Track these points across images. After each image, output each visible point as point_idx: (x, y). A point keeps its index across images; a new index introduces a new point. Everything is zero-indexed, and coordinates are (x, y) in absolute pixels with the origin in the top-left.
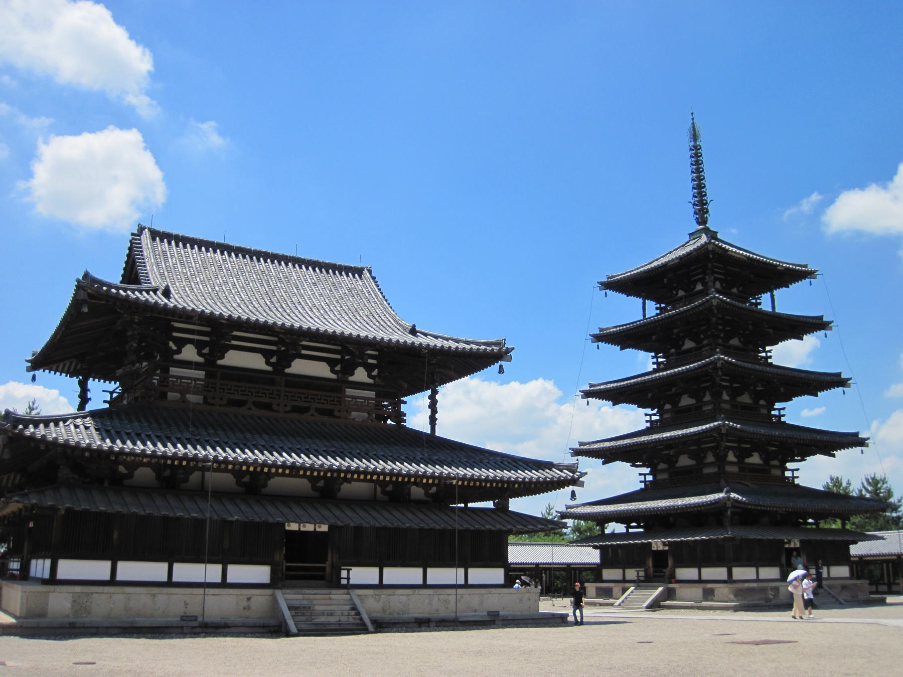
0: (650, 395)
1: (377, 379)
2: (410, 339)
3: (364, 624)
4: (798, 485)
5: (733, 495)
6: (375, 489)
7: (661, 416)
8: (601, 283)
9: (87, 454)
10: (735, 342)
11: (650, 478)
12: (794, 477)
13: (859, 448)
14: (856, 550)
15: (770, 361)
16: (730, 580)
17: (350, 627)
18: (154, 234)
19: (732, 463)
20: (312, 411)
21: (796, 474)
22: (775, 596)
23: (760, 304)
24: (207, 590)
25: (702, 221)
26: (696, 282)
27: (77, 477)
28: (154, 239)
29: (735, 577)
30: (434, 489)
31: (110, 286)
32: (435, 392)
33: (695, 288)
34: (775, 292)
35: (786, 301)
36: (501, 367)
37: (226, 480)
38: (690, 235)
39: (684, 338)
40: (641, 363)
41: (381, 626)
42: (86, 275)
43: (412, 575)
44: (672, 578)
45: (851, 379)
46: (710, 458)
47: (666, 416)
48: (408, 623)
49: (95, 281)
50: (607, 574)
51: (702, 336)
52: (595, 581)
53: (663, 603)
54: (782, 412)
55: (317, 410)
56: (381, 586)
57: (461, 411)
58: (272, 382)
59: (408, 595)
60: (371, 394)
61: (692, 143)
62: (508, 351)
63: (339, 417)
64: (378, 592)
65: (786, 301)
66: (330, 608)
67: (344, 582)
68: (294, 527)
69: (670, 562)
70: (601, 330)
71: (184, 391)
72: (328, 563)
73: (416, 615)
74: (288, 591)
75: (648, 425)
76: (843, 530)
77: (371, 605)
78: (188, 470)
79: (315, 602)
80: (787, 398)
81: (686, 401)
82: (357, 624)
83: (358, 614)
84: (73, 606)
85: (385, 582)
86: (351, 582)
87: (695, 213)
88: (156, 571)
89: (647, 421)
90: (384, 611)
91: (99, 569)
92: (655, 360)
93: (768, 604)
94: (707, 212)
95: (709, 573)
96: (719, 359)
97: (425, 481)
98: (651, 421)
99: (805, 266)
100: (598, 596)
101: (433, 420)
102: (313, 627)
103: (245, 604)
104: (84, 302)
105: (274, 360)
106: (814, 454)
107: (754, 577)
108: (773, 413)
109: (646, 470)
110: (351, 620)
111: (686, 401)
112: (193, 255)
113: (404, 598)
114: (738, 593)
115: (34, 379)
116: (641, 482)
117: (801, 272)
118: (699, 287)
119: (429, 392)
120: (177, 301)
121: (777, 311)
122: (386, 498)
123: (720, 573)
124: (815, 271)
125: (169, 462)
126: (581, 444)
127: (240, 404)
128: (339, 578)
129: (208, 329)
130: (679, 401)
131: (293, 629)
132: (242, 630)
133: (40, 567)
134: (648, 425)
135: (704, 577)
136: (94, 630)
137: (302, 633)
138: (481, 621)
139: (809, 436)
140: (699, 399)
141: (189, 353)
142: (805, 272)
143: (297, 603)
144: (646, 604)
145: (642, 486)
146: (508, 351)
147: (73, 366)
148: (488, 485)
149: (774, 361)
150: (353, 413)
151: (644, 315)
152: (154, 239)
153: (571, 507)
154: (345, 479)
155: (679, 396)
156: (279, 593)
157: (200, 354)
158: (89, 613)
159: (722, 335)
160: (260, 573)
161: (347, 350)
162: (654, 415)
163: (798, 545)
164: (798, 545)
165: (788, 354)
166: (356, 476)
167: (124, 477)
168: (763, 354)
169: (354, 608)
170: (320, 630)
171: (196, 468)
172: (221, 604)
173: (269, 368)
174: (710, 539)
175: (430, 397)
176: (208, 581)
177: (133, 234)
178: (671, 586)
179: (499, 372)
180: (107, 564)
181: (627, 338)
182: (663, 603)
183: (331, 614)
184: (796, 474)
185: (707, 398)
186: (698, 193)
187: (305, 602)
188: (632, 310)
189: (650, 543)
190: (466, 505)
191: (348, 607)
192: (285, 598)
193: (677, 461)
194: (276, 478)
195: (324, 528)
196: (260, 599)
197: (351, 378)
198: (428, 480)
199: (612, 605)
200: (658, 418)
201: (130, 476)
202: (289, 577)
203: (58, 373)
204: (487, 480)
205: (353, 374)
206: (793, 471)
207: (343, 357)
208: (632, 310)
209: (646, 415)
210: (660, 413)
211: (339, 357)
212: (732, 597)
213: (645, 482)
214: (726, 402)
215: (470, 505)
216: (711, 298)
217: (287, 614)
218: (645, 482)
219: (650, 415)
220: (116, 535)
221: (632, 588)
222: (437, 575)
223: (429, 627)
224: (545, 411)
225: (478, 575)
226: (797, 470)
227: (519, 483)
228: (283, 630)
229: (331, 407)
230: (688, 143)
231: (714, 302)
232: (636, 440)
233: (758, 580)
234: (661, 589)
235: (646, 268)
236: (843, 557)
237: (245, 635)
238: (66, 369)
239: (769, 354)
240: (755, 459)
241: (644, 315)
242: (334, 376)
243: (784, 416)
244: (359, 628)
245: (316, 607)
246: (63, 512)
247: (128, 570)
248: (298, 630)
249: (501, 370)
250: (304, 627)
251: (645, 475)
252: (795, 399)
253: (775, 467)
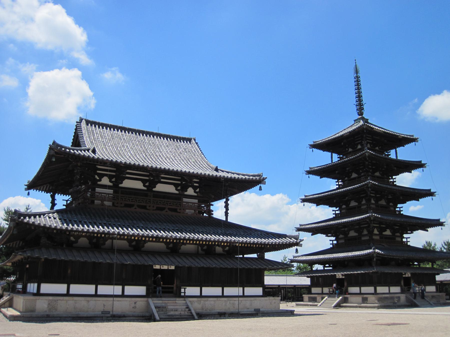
0: (335, 201)
1: (199, 194)
2: (215, 173)
3: (193, 315)
4: (409, 246)
5: (377, 250)
6: (198, 248)
7: (340, 211)
8: (310, 145)
9: (55, 231)
10: (377, 174)
11: (335, 242)
12: (407, 242)
13: (440, 227)
14: (439, 278)
15: (395, 183)
16: (375, 293)
17: (186, 317)
18: (88, 122)
19: (376, 235)
20: (166, 210)
21: (408, 240)
22: (398, 301)
23: (390, 155)
24: (115, 298)
25: (361, 114)
26: (358, 144)
27: (50, 242)
28: (87, 125)
29: (378, 292)
30: (227, 248)
31: (66, 148)
32: (227, 200)
33: (357, 147)
34: (397, 149)
35: (403, 154)
36: (260, 187)
37: (124, 244)
38: (355, 121)
39: (352, 172)
40: (330, 185)
41: (201, 316)
42: (54, 143)
43: (217, 291)
44: (346, 292)
45: (436, 192)
46: (365, 232)
47: (343, 211)
48: (215, 315)
49: (58, 145)
50: (314, 290)
51: (361, 171)
52: (308, 294)
53: (342, 305)
54: (401, 209)
56: (201, 296)
57: (240, 209)
58: (146, 195)
59: (214, 301)
60: (196, 201)
61: (355, 75)
62: (264, 179)
63: (180, 213)
64: (199, 299)
65: (403, 154)
66: (176, 307)
67: (183, 294)
68: (158, 267)
69: (346, 284)
70: (310, 168)
71: (103, 200)
72: (175, 285)
73: (218, 311)
74: (155, 299)
75: (334, 216)
76: (432, 268)
77: (197, 306)
78: (105, 239)
79: (168, 304)
80: (404, 202)
81: (353, 204)
82: (189, 315)
83: (190, 310)
84: (48, 306)
85: (203, 294)
86: (186, 294)
87: (357, 110)
88: (89, 289)
89: (333, 214)
90: (203, 309)
91: (61, 288)
92: (337, 183)
93: (395, 305)
94: (363, 109)
95: (365, 289)
96: (369, 182)
97: (223, 244)
98: (335, 214)
99: (413, 136)
100: (310, 301)
101: (227, 214)
102: (168, 317)
103: (133, 305)
104: (53, 156)
105: (147, 184)
106: (417, 230)
107: (388, 292)
108: (397, 209)
109: (334, 238)
110: (186, 313)
111: (353, 204)
112: (107, 132)
113: (213, 302)
114: (380, 300)
115: (29, 194)
116: (331, 244)
117: (411, 139)
118: (359, 147)
119: (225, 200)
120: (99, 155)
121: (398, 158)
122: (203, 253)
123: (371, 289)
124: (417, 139)
125: (95, 235)
126: (301, 225)
127: (131, 206)
128: (180, 292)
129: (115, 169)
130: (350, 204)
131: (158, 318)
132: (132, 318)
133: (32, 287)
134: (334, 216)
135: (362, 292)
136: (59, 318)
137: (162, 320)
139: (414, 221)
140: (359, 202)
141: (105, 181)
142: (412, 139)
143: (159, 305)
144: (333, 305)
145: (331, 246)
146: (264, 179)
147: (48, 188)
148: (254, 246)
149: (397, 183)
150: (187, 210)
151: (332, 161)
152: (87, 125)
153: (296, 257)
154: (183, 243)
155: (349, 201)
156: (150, 300)
157: (110, 181)
158: (56, 310)
159: (371, 171)
160: (141, 290)
161: (184, 179)
162: (337, 210)
163: (410, 276)
164: (410, 276)
165: (404, 180)
166: (188, 242)
167: (73, 242)
168: (392, 180)
170: (171, 318)
171: (109, 238)
172: (121, 306)
173: (145, 188)
174: (365, 273)
175: (225, 202)
176: (115, 294)
177: (77, 122)
178: (346, 296)
179: (260, 190)
180: (65, 286)
181: (323, 172)
182: (342, 305)
183: (176, 310)
184: (408, 240)
185: (364, 202)
186: (359, 100)
187: (163, 304)
188: (326, 158)
189: (335, 275)
190: (243, 256)
191: (185, 307)
192: (153, 302)
193: (349, 234)
195: (173, 268)
196: (141, 303)
197: (186, 193)
198: (224, 244)
199: (316, 305)
200: (339, 212)
201: (76, 242)
203: (41, 191)
204: (254, 243)
205: (186, 191)
206: (407, 238)
207: (182, 183)
208: (326, 158)
209: (333, 211)
210: (340, 210)
211: (179, 182)
212: (376, 301)
213: (333, 244)
214: (373, 204)
215: (245, 256)
216: (365, 152)
217: (155, 310)
218: (333, 244)
219: (335, 211)
220: (69, 271)
221: (326, 297)
222: (229, 291)
223: (225, 316)
224: (283, 209)
225: (249, 291)
226: (409, 238)
227: (270, 245)
228: (153, 318)
229: (176, 208)
230: (353, 75)
231: (367, 154)
232: (328, 223)
233: (389, 293)
234: (341, 298)
235: (332, 137)
236: (432, 282)
237: (133, 321)
238: (44, 189)
239: (394, 180)
240: (388, 232)
241: (332, 161)
242: (177, 192)
243: (402, 211)
244: (190, 317)
245: (169, 307)
246: (43, 260)
247: (76, 288)
248: (160, 318)
249: (260, 189)
250: (162, 316)
251: (333, 241)
252: (408, 203)
253: (398, 236)
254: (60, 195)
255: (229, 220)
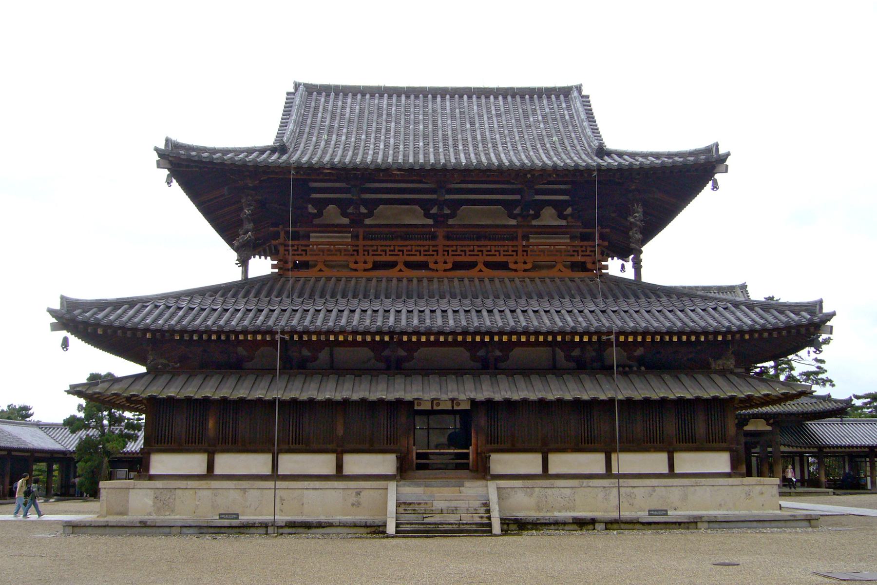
24: (278, 483)
27: (164, 361)
48: (565, 524)
55: (487, 265)
63: (516, 270)
66: (454, 504)
72: (471, 450)
82: (482, 525)
103: (353, 499)
110: (477, 520)
122: (573, 365)
125: (241, 337)
138: (675, 523)
156: (392, 486)
169: (486, 505)
194: (423, 350)
202: (420, 467)
229: (504, 259)
248: (397, 532)
254: (263, 257)
255: (646, 278)
